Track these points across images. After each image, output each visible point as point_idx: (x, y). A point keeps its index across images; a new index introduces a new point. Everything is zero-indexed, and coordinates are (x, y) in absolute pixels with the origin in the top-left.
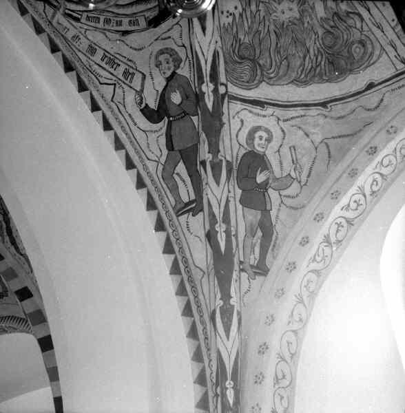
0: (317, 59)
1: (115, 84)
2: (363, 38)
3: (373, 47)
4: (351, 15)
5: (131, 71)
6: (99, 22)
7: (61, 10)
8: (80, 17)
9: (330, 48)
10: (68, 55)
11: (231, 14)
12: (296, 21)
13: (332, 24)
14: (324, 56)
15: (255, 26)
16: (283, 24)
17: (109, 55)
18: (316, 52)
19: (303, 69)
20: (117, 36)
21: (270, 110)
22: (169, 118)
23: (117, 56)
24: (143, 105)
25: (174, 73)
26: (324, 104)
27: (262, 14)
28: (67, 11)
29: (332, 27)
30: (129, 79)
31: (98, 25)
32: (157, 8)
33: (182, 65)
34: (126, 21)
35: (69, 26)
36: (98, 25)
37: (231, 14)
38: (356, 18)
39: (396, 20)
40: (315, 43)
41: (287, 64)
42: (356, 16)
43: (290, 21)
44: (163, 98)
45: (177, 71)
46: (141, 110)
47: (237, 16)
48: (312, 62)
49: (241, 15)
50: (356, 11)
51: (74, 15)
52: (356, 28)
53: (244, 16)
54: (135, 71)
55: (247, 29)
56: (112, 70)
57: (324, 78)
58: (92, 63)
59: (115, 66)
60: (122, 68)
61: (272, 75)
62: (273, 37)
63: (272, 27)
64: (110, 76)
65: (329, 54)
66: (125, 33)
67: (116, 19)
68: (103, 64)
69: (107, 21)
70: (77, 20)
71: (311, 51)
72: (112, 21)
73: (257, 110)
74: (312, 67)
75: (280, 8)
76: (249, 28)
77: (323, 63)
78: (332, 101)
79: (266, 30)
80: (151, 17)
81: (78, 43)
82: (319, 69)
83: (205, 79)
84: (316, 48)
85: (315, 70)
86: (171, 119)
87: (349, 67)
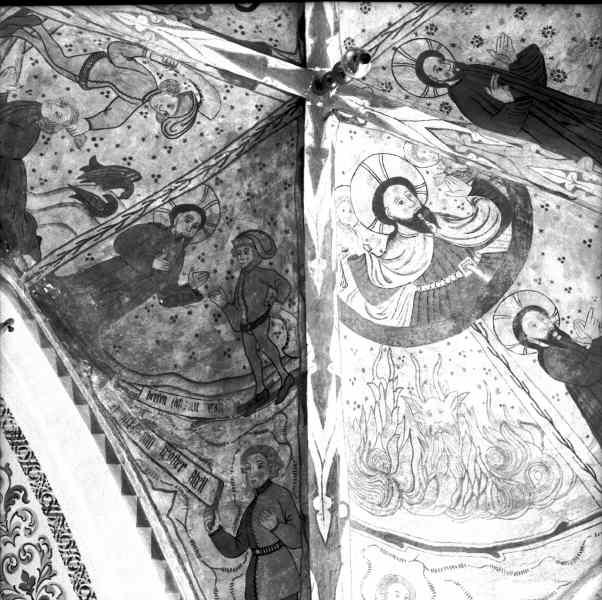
0: (479, 484)
1: (175, 492)
3: (561, 472)
4: (525, 426)
5: (203, 474)
9: (498, 469)
10: (113, 440)
11: (359, 406)
12: (449, 429)
13: (500, 437)
14: (490, 480)
15: (392, 428)
16: (431, 430)
18: (478, 472)
21: (409, 552)
22: (253, 550)
24: (215, 528)
25: (269, 483)
26: (493, 551)
27: (402, 411)
29: (499, 440)
30: (198, 486)
31: (163, 407)
32: (253, 391)
33: (283, 471)
38: (535, 431)
39: (591, 436)
40: (476, 461)
41: (435, 486)
42: (535, 429)
43: (440, 428)
44: (248, 517)
45: (273, 480)
46: (211, 536)
47: (368, 411)
48: (473, 487)
50: (532, 421)
52: (534, 444)
54: (208, 477)
55: (380, 430)
57: (491, 511)
59: (179, 466)
61: (415, 500)
63: (415, 433)
65: (499, 479)
73: (393, 548)
74: (472, 495)
75: (426, 407)
76: (383, 429)
77: (488, 491)
79: (407, 436)
82: (482, 498)
83: (320, 491)
85: (478, 498)
86: (258, 552)
87: (527, 498)
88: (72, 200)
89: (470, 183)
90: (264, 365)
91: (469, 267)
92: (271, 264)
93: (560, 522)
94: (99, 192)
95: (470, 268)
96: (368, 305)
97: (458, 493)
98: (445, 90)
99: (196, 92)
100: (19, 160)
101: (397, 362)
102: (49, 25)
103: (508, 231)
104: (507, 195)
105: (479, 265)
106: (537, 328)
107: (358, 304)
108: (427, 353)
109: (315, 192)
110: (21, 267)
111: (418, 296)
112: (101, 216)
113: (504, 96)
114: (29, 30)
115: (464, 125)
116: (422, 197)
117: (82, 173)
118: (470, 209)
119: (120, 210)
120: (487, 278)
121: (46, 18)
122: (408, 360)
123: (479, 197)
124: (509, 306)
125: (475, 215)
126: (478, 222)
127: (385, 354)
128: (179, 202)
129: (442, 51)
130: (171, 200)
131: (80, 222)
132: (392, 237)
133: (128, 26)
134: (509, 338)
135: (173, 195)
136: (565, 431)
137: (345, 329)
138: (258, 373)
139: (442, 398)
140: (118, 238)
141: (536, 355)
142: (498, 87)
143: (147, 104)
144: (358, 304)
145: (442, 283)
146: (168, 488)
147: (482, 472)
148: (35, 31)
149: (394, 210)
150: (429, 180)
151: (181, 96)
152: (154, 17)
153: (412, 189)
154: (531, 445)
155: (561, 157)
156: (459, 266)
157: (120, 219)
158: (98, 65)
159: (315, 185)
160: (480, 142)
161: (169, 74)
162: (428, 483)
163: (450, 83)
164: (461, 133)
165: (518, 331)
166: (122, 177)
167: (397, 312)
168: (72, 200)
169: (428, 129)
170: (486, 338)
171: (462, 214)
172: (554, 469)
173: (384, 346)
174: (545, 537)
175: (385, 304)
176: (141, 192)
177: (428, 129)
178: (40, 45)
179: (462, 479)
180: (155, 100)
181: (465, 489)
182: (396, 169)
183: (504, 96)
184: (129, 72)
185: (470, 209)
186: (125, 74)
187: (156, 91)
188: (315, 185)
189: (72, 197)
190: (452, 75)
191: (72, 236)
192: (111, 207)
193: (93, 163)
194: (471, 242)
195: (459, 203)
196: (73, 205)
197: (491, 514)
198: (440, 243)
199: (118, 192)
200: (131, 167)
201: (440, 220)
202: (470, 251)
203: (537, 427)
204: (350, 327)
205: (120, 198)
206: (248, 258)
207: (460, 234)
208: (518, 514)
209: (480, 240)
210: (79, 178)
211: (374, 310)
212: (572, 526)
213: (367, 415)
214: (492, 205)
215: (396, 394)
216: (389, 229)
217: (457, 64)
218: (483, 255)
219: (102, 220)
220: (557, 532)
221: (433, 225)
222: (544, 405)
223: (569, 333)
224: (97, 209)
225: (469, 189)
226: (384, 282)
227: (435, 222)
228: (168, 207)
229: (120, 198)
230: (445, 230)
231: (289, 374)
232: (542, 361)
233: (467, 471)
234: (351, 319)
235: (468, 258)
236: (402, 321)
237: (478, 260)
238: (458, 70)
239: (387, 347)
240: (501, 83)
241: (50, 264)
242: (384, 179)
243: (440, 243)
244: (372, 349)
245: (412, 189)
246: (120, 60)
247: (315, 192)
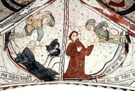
6: (111, 70)
7: (97, 77)
8: (104, 74)
17: (123, 75)
20: (120, 68)
23: (126, 73)
28: (99, 76)
34: (118, 61)
35: (103, 79)
36: (111, 71)
51: (102, 75)
56: (129, 78)
58: (121, 82)
59: (128, 76)
60: (131, 74)
64: (130, 80)
66: (121, 64)
67: (115, 64)
68: (124, 79)
69: (113, 67)
70: (105, 75)
72: (114, 66)
80: (124, 52)
81: (111, 81)
88: (51, 58)
90: (119, 40)
94: (54, 51)
96: (123, 7)
99: (48, 12)
100: (35, 61)
102: (12, 31)
107: (121, 9)
110: (57, 79)
112: (59, 54)
114: (11, 36)
117: (47, 51)
119: (61, 49)
121: (11, 30)
128: (68, 35)
130: (67, 36)
131: (56, 59)
133: (25, 14)
135: (66, 36)
138: (120, 43)
140: (67, 54)
143: (43, 25)
144: (121, 9)
146: (132, 82)
148: (11, 35)
151: (46, 17)
152: (27, 7)
157: (63, 50)
158: (28, 29)
161: (41, 15)
166: (55, 43)
168: (51, 58)
175: (126, 4)
176: (60, 41)
178: (15, 36)
180: (44, 22)
184: (34, 23)
186: (34, 24)
187: (42, 21)
189: (50, 57)
191: (59, 64)
192: (59, 51)
193: (48, 47)
196: (52, 58)
199: (57, 46)
200: (54, 40)
205: (59, 46)
206: (92, 28)
210: (48, 52)
211: (125, 7)
219: (60, 55)
224: (57, 54)
228: (68, 38)
229: (59, 46)
231: (126, 35)
236: (133, 3)
241: (61, 73)
246: (30, 23)
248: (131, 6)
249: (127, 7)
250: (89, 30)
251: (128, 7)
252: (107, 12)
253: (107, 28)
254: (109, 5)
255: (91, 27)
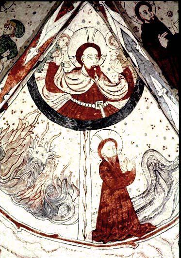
2: (71, 205)
3: (73, 215)
4: (74, 187)
11: (8, 124)
13: (60, 184)
15: (15, 145)
16: (32, 159)
18: (38, 191)
19: (23, 194)
26: (19, 225)
27: (25, 142)
29: (58, 185)
37: (8, 124)
38: (76, 192)
39: (97, 209)
40: (41, 186)
47: (11, 129)
49: (13, 131)
50: (78, 188)
53: (14, 133)
55: (10, 141)
62: (21, 160)
63: (24, 155)
71: (36, 189)
75: (37, 149)
77: (37, 200)
78: (24, 226)
84: (40, 189)
89: (124, 68)
91: (100, 106)
92: (16, 40)
93: (56, 234)
95: (99, 106)
96: (45, 88)
97: (23, 192)
98: (142, 23)
101: (39, 121)
103: (125, 102)
104: (135, 84)
105: (104, 109)
106: (108, 152)
108: (55, 128)
109: (55, 21)
111: (70, 102)
113: (164, 43)
115: (138, 41)
116: (101, 61)
118: (117, 81)
120: (104, 116)
122: (45, 123)
123: (123, 77)
124: (104, 133)
125: (117, 84)
126: (115, 89)
127: (36, 114)
129: (153, 7)
132: (77, 69)
134: (95, 147)
136: (88, 202)
137: (26, 88)
139: (48, 151)
141: (101, 162)
142: (165, 37)
144: (41, 84)
145: (84, 104)
147: (40, 192)
149: (85, 58)
150: (108, 57)
153: (100, 55)
154: (70, 197)
155: (167, 82)
156: (96, 102)
159: (57, 19)
160: (138, 51)
162: (13, 179)
163: (146, 22)
164: (133, 41)
165: (101, 146)
167: (55, 101)
169: (122, 30)
170: (85, 141)
171: (112, 80)
172: (72, 212)
173: (39, 110)
174: (45, 235)
175: (53, 94)
177: (122, 30)
179: (30, 188)
181: (27, 192)
182: (99, 41)
183: (164, 43)
185: (117, 81)
188: (57, 19)
190: (149, 19)
194: (109, 96)
195: (114, 75)
197: (30, 210)
198: (95, 85)
201: (102, 75)
202: (105, 99)
203: (79, 191)
204: (30, 91)
206: (8, 32)
207: (106, 88)
208: (41, 219)
209: (112, 98)
211: (46, 92)
212: (60, 239)
213: (8, 131)
214: (127, 85)
215: (29, 133)
216: (78, 65)
217: (155, 16)
218: (109, 105)
220: (52, 236)
221: (98, 78)
222: (88, 184)
223: (120, 161)
225: (121, 71)
226: (59, 83)
227: (99, 76)
230: (101, 83)
232: (101, 165)
233: (34, 187)
234: (33, 88)
235: (102, 101)
236: (55, 107)
237: (105, 105)
238: (153, 19)
239: (40, 112)
240: (166, 37)
242: (90, 41)
243: (95, 85)
244: (32, 107)
245: (100, 55)
247: (55, 21)
248: (48, 103)
249: (45, 96)
250: (6, 26)
251: (47, 97)
252: (29, 55)
253: (6, 58)
254: (49, 61)
255: (12, 31)
